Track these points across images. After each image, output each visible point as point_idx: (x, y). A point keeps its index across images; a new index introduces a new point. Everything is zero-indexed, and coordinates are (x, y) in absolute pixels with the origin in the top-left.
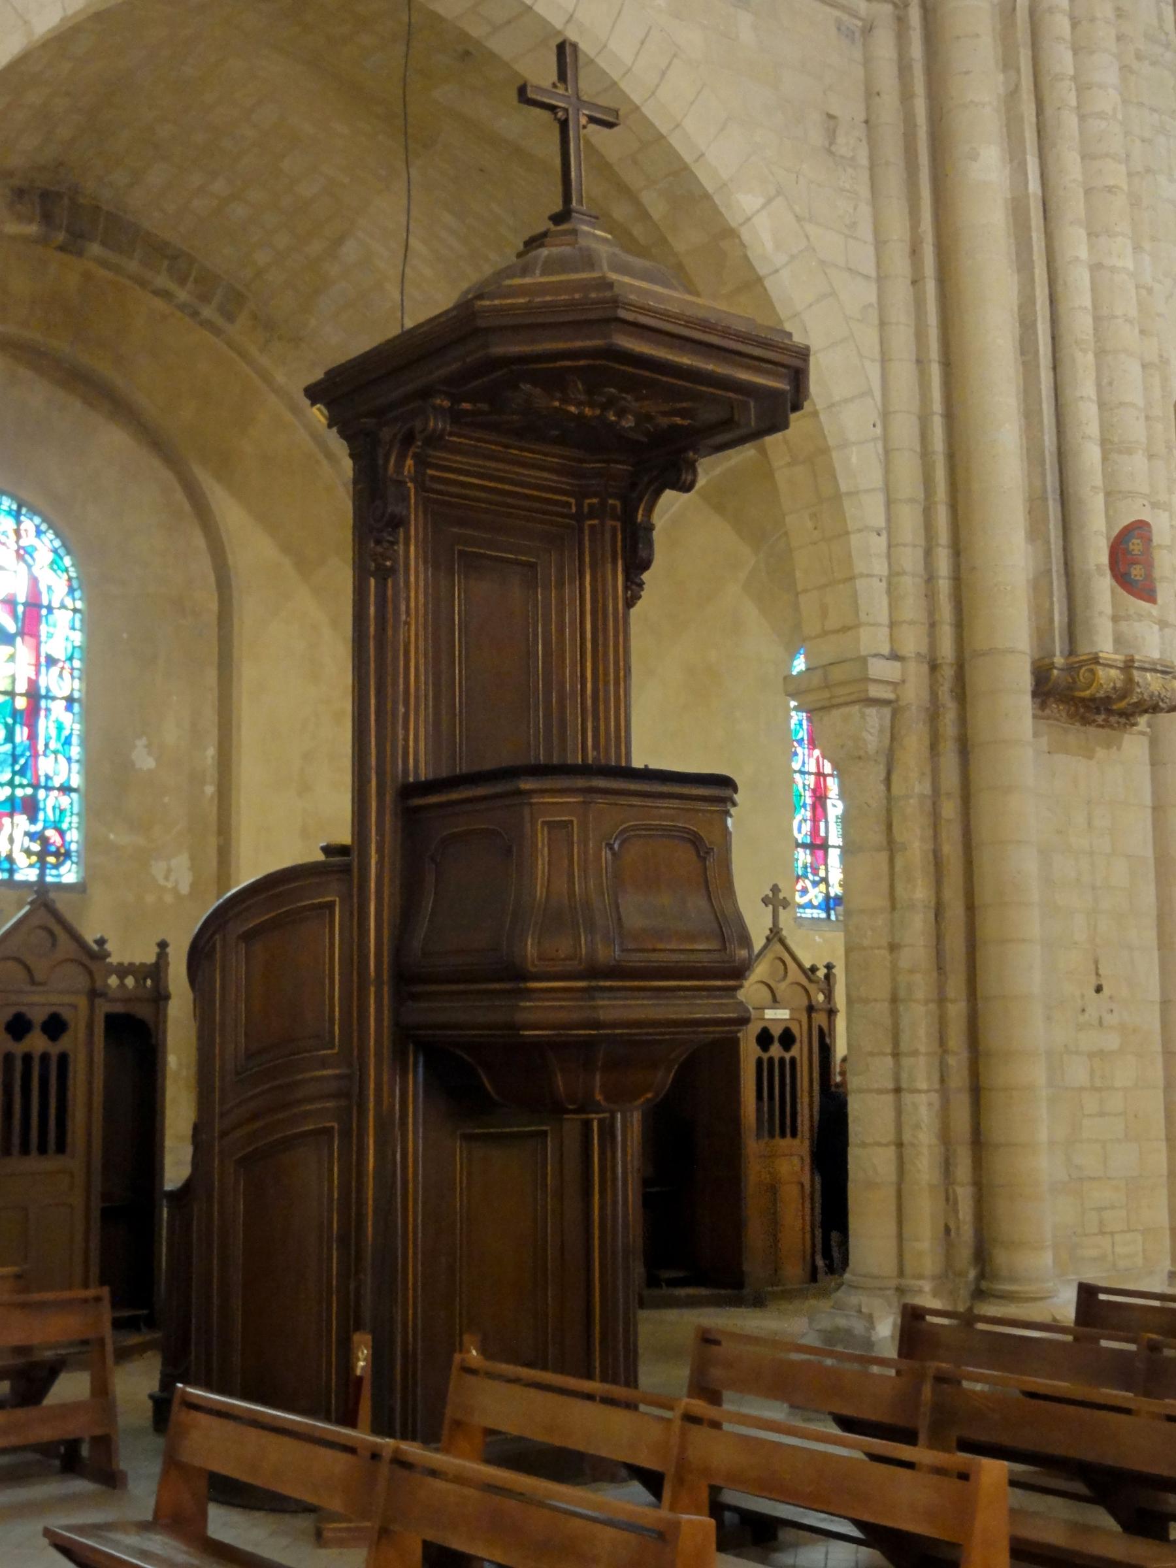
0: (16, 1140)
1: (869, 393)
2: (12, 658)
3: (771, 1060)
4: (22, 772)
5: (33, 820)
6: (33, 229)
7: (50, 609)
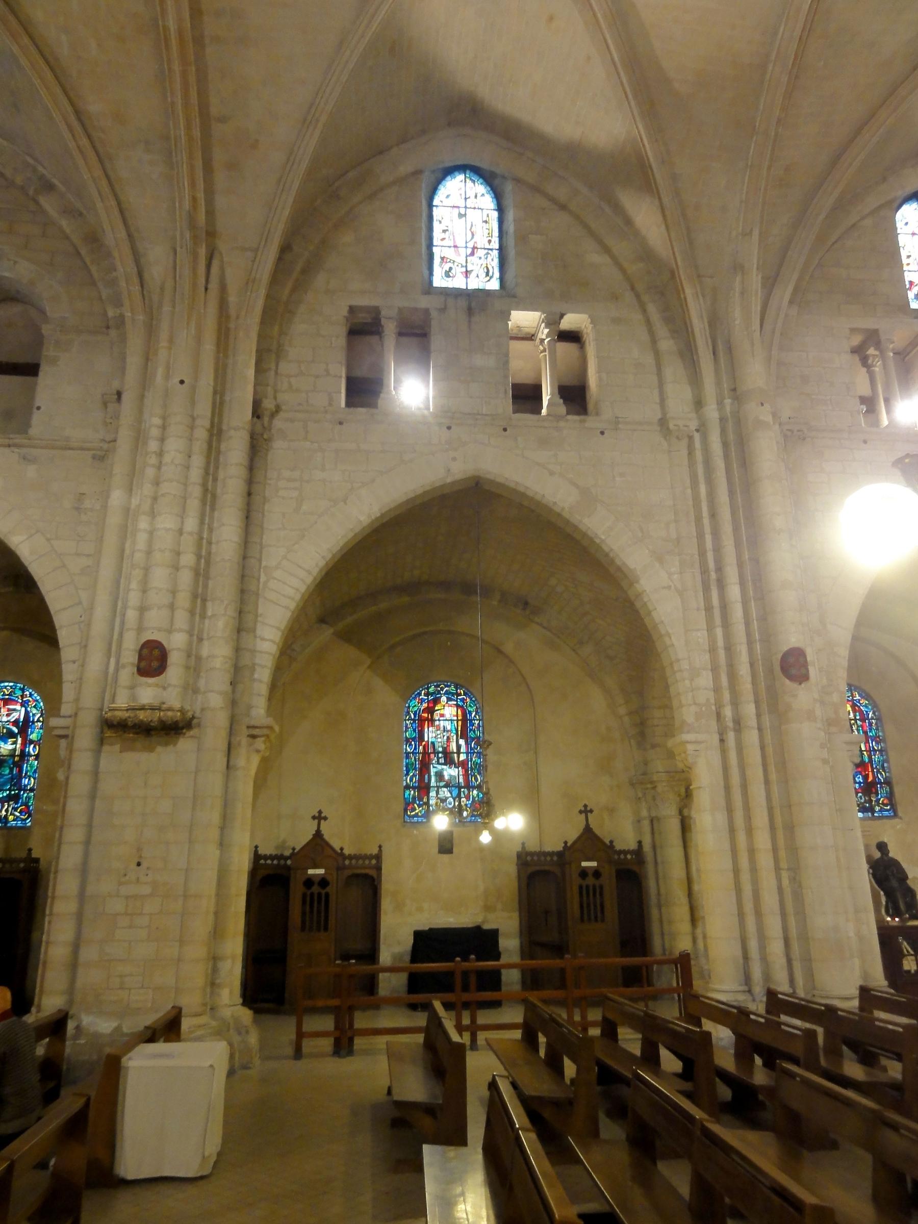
0: (593, 917)
1: (80, 603)
2: (15, 743)
3: (312, 895)
4: (15, 785)
5: (16, 803)
6: (11, 589)
7: (33, 722)
